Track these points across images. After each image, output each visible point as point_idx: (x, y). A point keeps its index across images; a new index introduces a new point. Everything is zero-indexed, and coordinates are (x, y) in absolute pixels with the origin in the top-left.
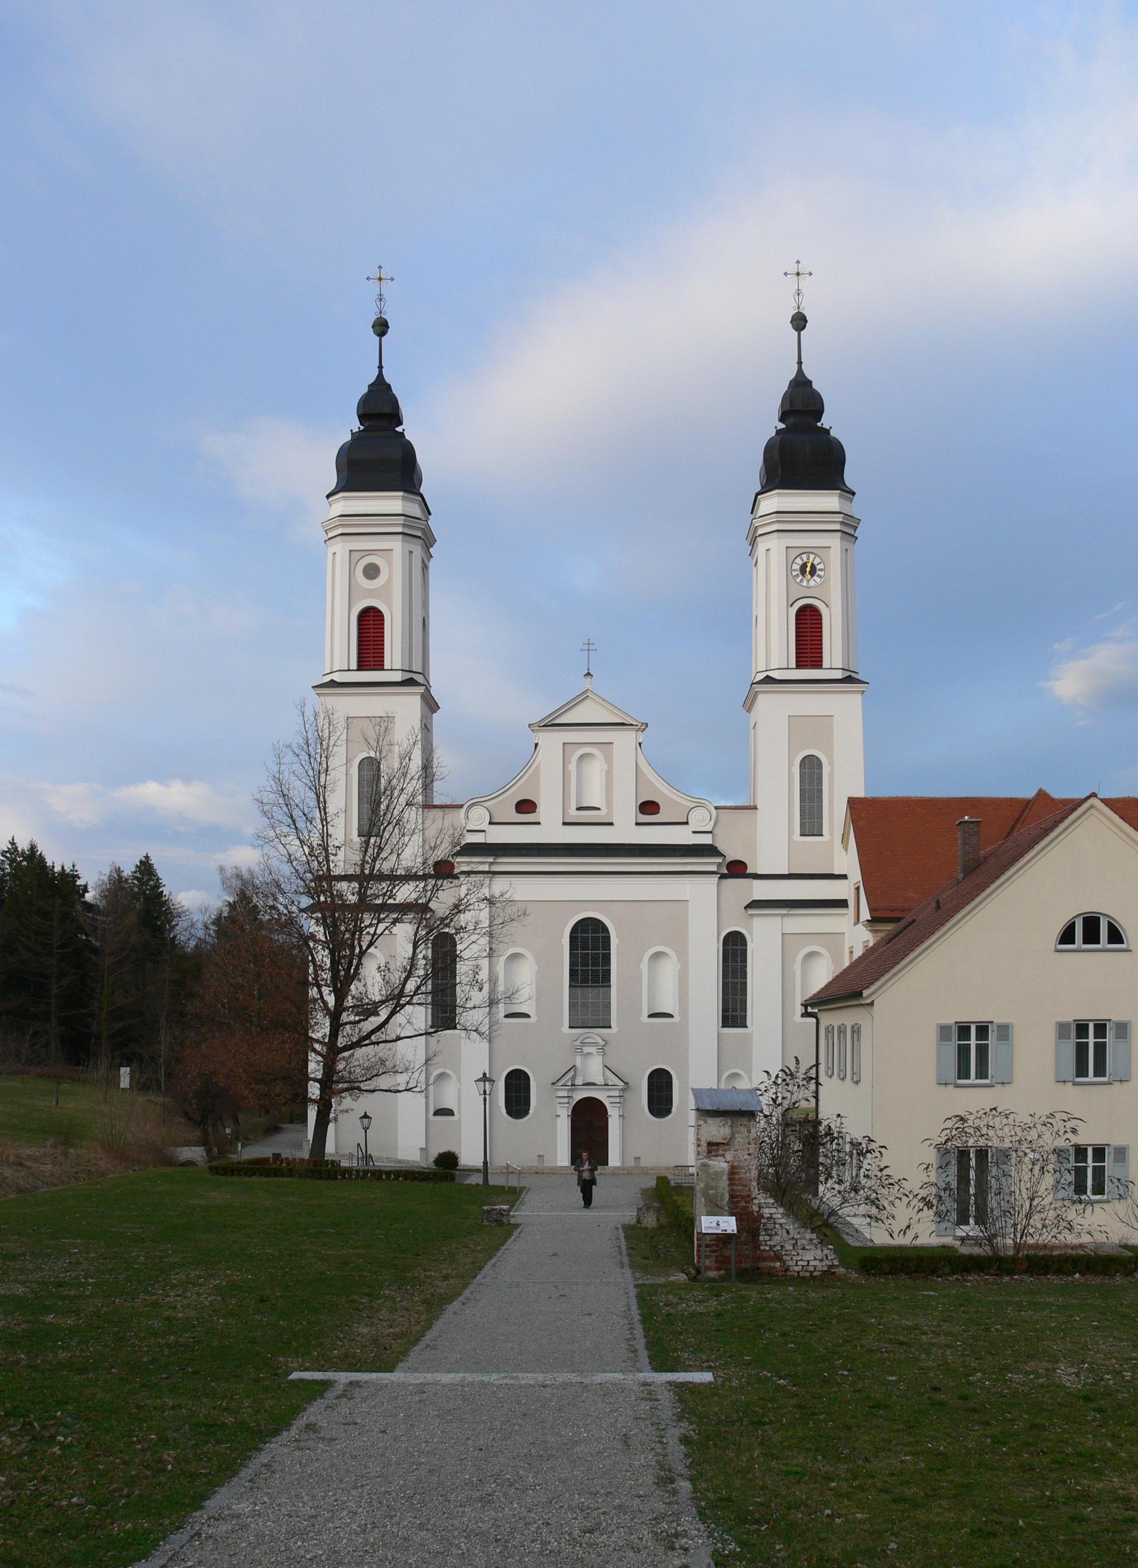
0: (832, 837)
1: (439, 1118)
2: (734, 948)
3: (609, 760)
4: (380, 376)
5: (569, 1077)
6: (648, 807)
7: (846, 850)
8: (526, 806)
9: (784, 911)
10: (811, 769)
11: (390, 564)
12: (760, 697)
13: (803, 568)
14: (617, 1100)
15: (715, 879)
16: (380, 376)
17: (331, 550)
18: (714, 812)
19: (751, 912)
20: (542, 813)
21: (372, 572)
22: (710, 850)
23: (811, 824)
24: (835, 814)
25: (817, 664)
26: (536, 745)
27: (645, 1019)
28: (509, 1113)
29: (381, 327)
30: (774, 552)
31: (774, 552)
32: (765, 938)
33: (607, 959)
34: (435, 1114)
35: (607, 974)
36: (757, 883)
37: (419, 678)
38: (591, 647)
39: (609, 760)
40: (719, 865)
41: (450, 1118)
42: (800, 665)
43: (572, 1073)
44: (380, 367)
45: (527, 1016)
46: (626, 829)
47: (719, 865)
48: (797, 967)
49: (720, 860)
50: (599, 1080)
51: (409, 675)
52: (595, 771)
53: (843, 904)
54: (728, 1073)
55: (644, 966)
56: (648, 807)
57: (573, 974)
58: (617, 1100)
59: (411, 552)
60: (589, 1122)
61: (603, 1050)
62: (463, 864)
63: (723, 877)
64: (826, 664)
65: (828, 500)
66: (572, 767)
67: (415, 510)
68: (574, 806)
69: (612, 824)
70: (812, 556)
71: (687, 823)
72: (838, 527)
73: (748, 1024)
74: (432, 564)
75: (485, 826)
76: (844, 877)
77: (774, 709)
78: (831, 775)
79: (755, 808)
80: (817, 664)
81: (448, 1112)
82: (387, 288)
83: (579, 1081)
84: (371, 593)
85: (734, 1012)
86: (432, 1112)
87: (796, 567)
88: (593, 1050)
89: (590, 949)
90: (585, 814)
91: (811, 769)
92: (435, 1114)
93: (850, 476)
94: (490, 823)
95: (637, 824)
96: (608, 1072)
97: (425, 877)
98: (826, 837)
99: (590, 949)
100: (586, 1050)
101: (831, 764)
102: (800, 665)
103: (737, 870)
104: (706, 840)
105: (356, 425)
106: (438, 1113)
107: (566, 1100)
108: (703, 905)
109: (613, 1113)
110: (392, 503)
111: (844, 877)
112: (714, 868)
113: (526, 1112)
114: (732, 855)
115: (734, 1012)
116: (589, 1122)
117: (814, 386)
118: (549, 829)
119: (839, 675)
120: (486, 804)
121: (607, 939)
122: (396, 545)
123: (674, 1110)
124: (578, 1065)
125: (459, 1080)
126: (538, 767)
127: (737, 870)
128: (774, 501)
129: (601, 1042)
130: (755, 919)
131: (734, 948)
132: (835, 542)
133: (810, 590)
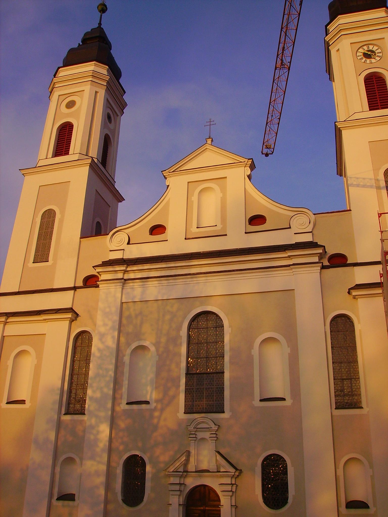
3: (223, 190)
6: (257, 220)
11: (82, 98)
14: (229, 488)
15: (317, 268)
19: (354, 293)
22: (312, 245)
26: (168, 186)
27: (257, 403)
34: (58, 499)
38: (212, 123)
40: (321, 256)
41: (71, 503)
49: (320, 251)
58: (229, 488)
59: (96, 92)
62: (105, 275)
66: (195, 198)
68: (195, 225)
69: (226, 235)
71: (290, 228)
73: (364, 404)
75: (125, 246)
79: (350, 210)
81: (70, 497)
83: (191, 467)
84: (68, 115)
88: (207, 435)
92: (58, 499)
94: (128, 243)
95: (246, 233)
96: (219, 457)
97: (75, 288)
100: (200, 435)
103: (339, 261)
104: (307, 238)
107: (177, 487)
112: (316, 259)
120: (127, 231)
123: (290, 500)
124: (193, 452)
126: (168, 202)
127: (339, 261)
129: (215, 428)
130: (360, 301)
131: (342, 328)
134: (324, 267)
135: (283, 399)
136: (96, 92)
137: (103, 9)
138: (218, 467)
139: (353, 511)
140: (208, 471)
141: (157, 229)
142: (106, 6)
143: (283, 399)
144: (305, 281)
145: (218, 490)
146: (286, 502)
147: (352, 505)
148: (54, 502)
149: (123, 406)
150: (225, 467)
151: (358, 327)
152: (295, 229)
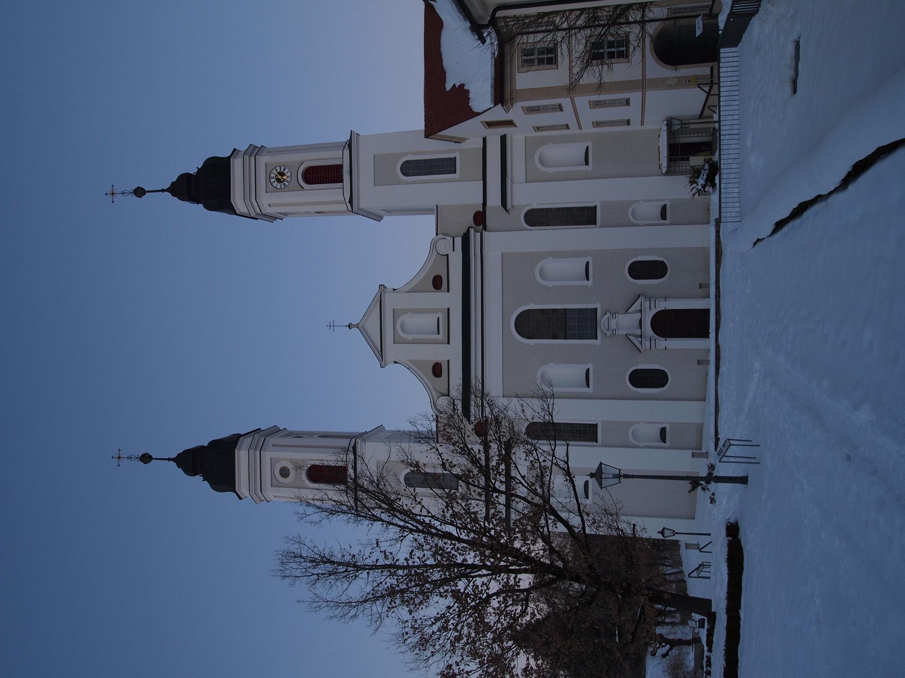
0: (457, 150)
1: (668, 439)
2: (538, 218)
3: (404, 312)
4: (173, 460)
5: (632, 341)
6: (437, 283)
7: (466, 139)
8: (437, 370)
9: (509, 182)
10: (412, 168)
12: (361, 206)
13: (279, 181)
14: (653, 302)
16: (173, 460)
17: (273, 498)
18: (440, 236)
19: (509, 206)
21: (284, 472)
22: (466, 239)
23: (446, 166)
24: (435, 149)
25: (340, 167)
27: (589, 283)
28: (663, 385)
29: (146, 458)
30: (269, 201)
31: (269, 201)
32: (527, 196)
34: (664, 442)
36: (489, 204)
39: (404, 312)
40: (476, 231)
41: (668, 430)
43: (632, 338)
44: (169, 459)
45: (588, 370)
46: (452, 299)
47: (476, 231)
48: (550, 170)
49: (472, 231)
50: (638, 316)
51: (351, 449)
52: (411, 320)
53: (503, 139)
54: (631, 219)
55: (550, 284)
56: (437, 283)
59: (274, 445)
60: (670, 324)
61: (614, 314)
63: (485, 228)
64: (340, 163)
65: (237, 167)
66: (410, 337)
67: (246, 442)
68: (436, 336)
70: (272, 175)
71: (447, 255)
72: (253, 158)
73: (593, 205)
74: (291, 428)
76: (484, 139)
77: (369, 196)
78: (413, 154)
80: (340, 167)
81: (663, 431)
82: (124, 454)
83: (638, 332)
85: (584, 216)
86: (663, 444)
87: (279, 186)
89: (533, 324)
90: (443, 327)
91: (412, 168)
92: (664, 442)
94: (448, 395)
98: (456, 155)
99: (533, 324)
100: (613, 326)
101: (406, 154)
103: (480, 218)
104: (458, 241)
105: (199, 478)
106: (664, 440)
107: (653, 342)
109: (662, 305)
110: (242, 456)
111: (484, 139)
112: (478, 234)
113: (663, 372)
114: (470, 221)
115: (584, 216)
116: (670, 324)
117: (175, 180)
118: (452, 354)
119: (347, 152)
121: (528, 312)
122: (268, 455)
123: (660, 259)
124: (625, 332)
125: (637, 423)
126: (411, 361)
127: (480, 218)
128: (238, 201)
131: (538, 218)
132: (263, 160)
133: (295, 176)
134: (485, 228)
135: (588, 263)
136: (274, 445)
137: (146, 458)
138: (637, 311)
139: (668, 215)
140: (641, 320)
141: (437, 370)
142: (144, 455)
143: (588, 263)
144: (497, 245)
145: (654, 311)
146: (663, 262)
147: (663, 216)
148: (667, 444)
149: (590, 390)
150: (636, 306)
151: (535, 206)
152: (450, 252)
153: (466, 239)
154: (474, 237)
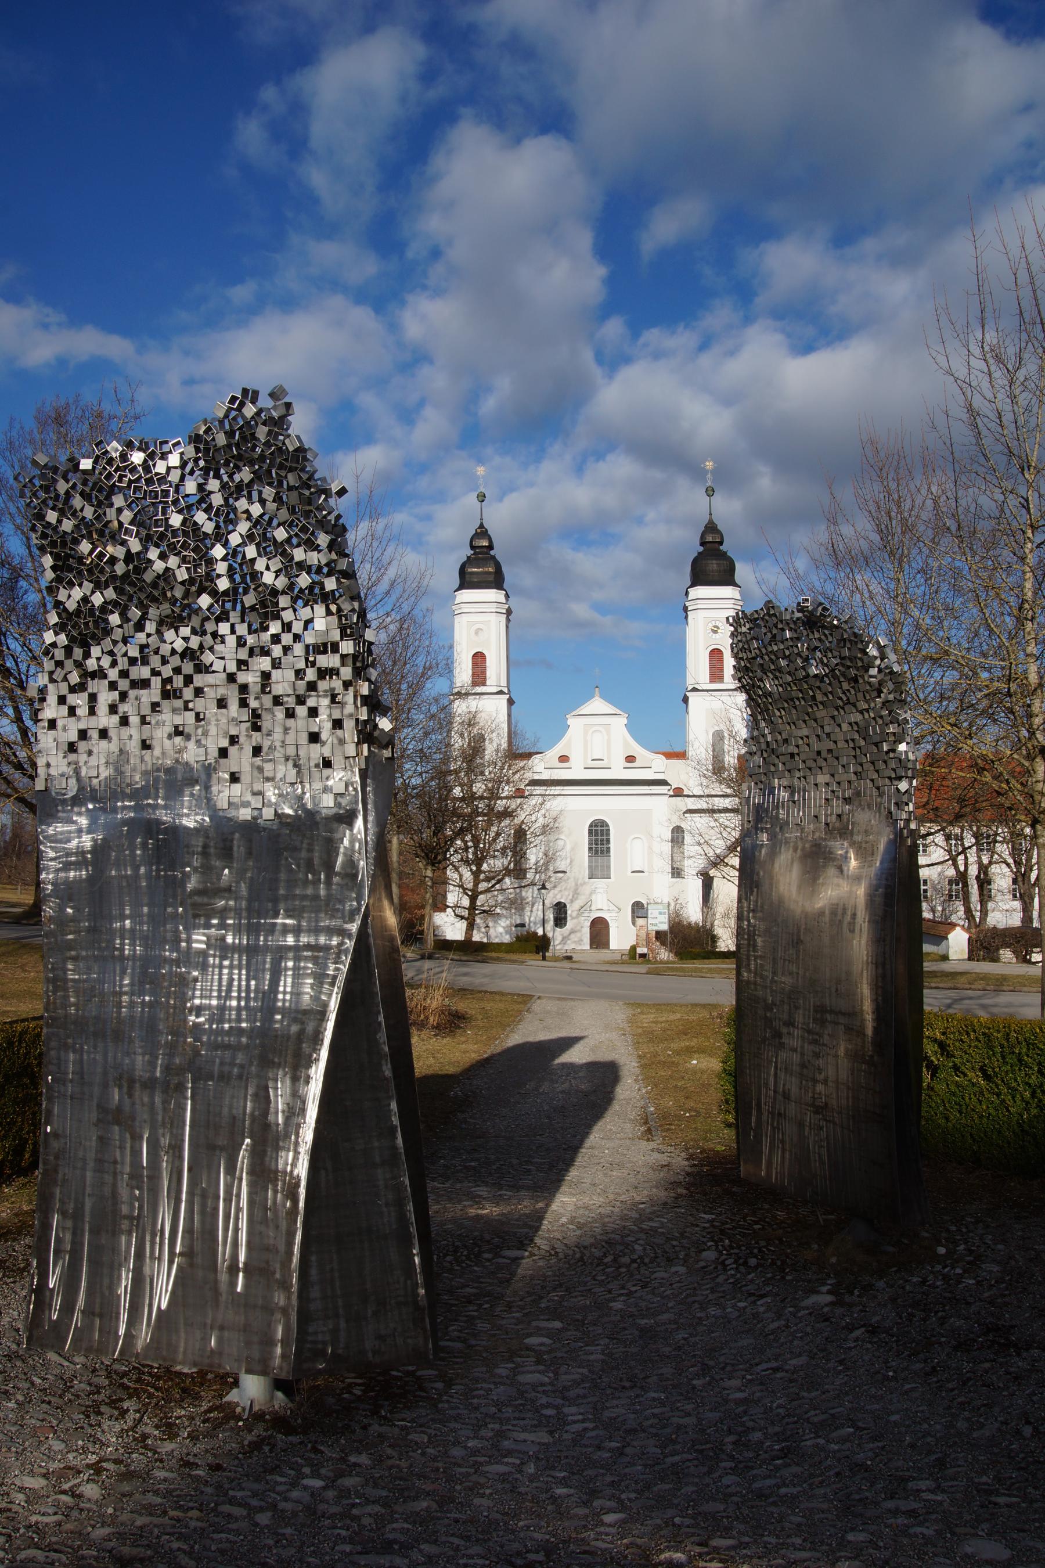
2: (678, 834)
4: (481, 526)
6: (630, 759)
16: (481, 526)
20: (572, 763)
22: (663, 783)
33: (608, 841)
35: (608, 849)
37: (505, 690)
42: (712, 681)
56: (630, 759)
57: (590, 849)
60: (599, 931)
89: (599, 836)
93: (737, 578)
102: (712, 681)
103: (678, 793)
108: (661, 811)
127: (678, 793)
141: (564, 759)
153: (663, 783)
154: (663, 789)
